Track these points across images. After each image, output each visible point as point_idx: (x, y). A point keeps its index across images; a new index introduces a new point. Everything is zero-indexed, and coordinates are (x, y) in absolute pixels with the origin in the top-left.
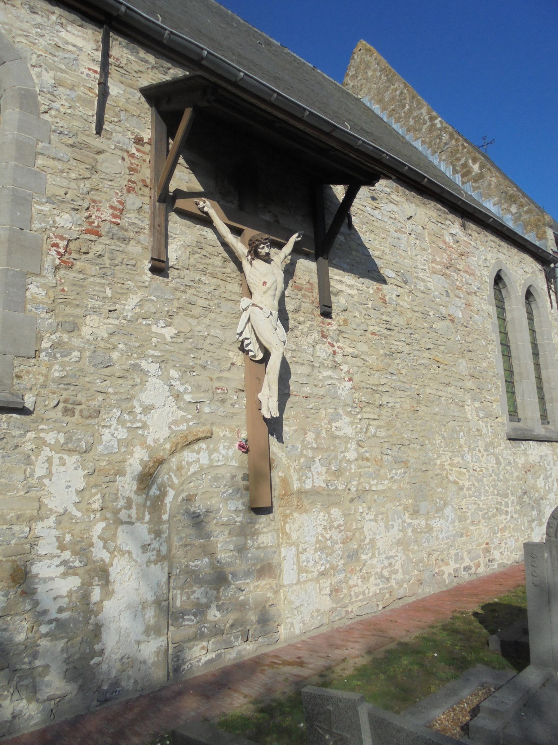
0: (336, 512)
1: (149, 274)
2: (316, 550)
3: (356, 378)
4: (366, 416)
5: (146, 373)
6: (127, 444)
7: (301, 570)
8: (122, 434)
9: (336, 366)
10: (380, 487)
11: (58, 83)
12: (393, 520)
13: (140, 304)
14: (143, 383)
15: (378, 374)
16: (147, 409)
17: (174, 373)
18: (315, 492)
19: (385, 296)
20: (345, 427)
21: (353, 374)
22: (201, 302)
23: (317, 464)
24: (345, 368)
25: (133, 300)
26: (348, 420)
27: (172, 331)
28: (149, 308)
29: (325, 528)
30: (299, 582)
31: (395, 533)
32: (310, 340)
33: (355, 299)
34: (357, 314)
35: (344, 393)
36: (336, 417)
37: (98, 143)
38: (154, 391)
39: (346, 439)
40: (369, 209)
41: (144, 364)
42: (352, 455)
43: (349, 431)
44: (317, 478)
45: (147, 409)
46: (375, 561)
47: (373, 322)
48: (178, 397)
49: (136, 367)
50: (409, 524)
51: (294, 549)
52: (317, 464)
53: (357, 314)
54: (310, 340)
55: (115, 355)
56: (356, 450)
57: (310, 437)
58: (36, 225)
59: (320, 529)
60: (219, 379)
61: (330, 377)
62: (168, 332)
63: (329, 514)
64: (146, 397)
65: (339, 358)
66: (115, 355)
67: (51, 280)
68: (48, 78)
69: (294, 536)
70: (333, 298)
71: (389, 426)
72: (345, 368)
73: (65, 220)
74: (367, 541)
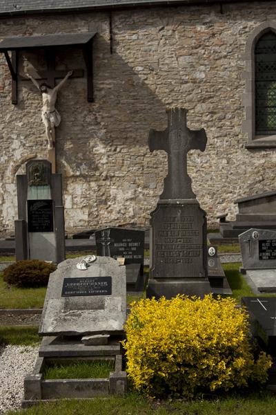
0: (93, 184)
1: (13, 106)
2: (81, 198)
3: (110, 127)
4: (115, 143)
5: (13, 139)
6: (7, 161)
7: (73, 204)
8: (6, 158)
9: (98, 124)
10: (121, 175)
12: (129, 189)
13: (11, 117)
14: (12, 142)
16: (14, 150)
17: (22, 138)
19: (134, 82)
22: (32, 111)
24: (102, 124)
25: (9, 116)
26: (102, 146)
27: (22, 123)
28: (14, 117)
30: (72, 208)
31: (129, 195)
32: (83, 115)
33: (112, 89)
38: (16, 144)
41: (12, 136)
43: (103, 151)
45: (14, 150)
46: (116, 206)
47: (124, 98)
48: (24, 145)
49: (10, 138)
50: (140, 192)
51: (71, 196)
53: (112, 97)
54: (83, 115)
55: (4, 135)
57: (80, 155)
59: (84, 190)
60: (40, 137)
61: (93, 129)
62: (20, 124)
63: (89, 185)
64: (13, 146)
65: (99, 120)
66: (4, 135)
69: (71, 191)
70: (96, 93)
72: (102, 124)
74: (111, 197)
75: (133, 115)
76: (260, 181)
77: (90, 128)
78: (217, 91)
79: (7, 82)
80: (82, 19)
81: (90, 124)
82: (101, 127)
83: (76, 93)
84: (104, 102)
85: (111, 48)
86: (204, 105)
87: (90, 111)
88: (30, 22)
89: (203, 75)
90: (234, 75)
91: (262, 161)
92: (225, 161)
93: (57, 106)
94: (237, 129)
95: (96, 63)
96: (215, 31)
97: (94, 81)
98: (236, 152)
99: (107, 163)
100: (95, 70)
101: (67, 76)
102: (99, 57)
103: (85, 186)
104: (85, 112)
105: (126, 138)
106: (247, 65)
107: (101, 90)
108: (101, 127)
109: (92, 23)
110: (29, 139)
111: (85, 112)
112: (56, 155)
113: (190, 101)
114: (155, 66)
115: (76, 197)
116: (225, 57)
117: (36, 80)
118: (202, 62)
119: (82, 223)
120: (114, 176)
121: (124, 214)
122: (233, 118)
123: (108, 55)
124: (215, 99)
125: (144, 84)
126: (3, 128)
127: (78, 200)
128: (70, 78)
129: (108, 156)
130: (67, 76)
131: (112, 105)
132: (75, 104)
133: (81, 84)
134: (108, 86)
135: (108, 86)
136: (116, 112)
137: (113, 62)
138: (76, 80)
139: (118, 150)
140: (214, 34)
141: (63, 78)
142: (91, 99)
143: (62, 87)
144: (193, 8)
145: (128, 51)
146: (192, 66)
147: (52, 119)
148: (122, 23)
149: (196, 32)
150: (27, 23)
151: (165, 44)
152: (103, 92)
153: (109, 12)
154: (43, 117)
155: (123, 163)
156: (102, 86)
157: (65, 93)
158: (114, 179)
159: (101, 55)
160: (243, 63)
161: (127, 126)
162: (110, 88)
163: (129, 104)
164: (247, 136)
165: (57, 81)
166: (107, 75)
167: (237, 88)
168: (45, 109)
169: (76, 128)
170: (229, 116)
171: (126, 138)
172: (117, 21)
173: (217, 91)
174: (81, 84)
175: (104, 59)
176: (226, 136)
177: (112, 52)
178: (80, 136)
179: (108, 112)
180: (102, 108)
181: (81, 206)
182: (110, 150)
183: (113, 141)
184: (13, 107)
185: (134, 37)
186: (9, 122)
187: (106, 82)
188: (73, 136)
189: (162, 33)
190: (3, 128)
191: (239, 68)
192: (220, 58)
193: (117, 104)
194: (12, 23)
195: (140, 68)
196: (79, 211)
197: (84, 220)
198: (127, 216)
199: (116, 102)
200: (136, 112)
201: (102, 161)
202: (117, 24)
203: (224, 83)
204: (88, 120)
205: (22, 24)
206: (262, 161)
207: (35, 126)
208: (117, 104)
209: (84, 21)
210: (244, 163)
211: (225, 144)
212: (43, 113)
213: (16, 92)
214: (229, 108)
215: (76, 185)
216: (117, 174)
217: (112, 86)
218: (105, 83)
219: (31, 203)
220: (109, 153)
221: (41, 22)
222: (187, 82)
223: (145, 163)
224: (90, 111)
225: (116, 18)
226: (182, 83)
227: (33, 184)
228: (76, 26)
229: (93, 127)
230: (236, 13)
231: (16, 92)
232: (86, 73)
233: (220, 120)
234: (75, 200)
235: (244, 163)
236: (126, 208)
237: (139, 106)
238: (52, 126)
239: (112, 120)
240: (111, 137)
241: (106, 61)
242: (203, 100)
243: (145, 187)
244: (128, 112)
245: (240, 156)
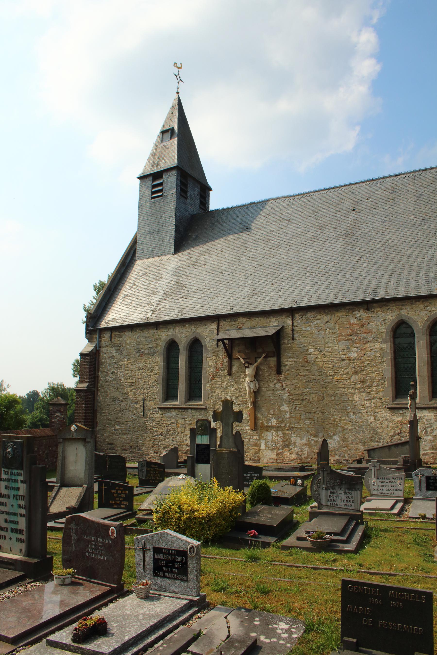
0: (280, 433)
2: (272, 442)
3: (292, 392)
4: (295, 404)
7: (266, 446)
9: (284, 389)
10: (299, 426)
11: (210, 339)
12: (304, 437)
13: (227, 384)
15: (302, 389)
18: (272, 427)
19: (308, 360)
20: (285, 408)
21: (290, 391)
23: (273, 419)
24: (287, 389)
26: (286, 405)
27: (234, 388)
28: (229, 384)
29: (275, 436)
30: (266, 449)
31: (304, 441)
32: (273, 383)
34: (293, 370)
35: (285, 397)
36: (282, 405)
37: (217, 349)
39: (286, 412)
40: (304, 328)
42: (288, 416)
43: (287, 409)
44: (274, 422)
46: (295, 449)
47: (301, 371)
50: (312, 440)
51: (264, 441)
52: (273, 419)
53: (293, 370)
54: (273, 383)
56: (290, 415)
57: (271, 411)
58: (207, 373)
59: (273, 437)
61: (280, 393)
62: (233, 389)
63: (277, 433)
65: (284, 387)
66: (222, 396)
67: (210, 384)
68: (208, 340)
69: (265, 437)
70: (282, 368)
71: (305, 407)
72: (287, 389)
73: (212, 369)
74: (292, 442)
75: (307, 384)
76: (398, 434)
77: (278, 392)
78: (365, 366)
79: (225, 360)
80: (274, 317)
81: (278, 390)
82: (286, 391)
83: (269, 368)
84: (288, 374)
85: (293, 337)
86: (357, 377)
87: (278, 380)
88: (241, 320)
89: (356, 355)
90: (378, 354)
91: (400, 418)
92: (372, 418)
93: (257, 376)
94: (381, 394)
95: (283, 347)
96: (363, 322)
97: (281, 359)
98: (381, 411)
99: (289, 418)
100: (282, 353)
101: (263, 357)
102: (284, 343)
103: (274, 434)
104: (275, 381)
105: (303, 400)
106: (388, 347)
107: (286, 365)
108: (286, 391)
109: (281, 320)
110: (238, 399)
111: (275, 381)
112: (255, 411)
113: (347, 373)
114: (322, 348)
115: (268, 442)
116: (371, 341)
117: (243, 358)
118: (355, 345)
119: (272, 461)
120: (294, 427)
121: (301, 455)
122: (378, 385)
123: (291, 341)
124: (365, 372)
125: (315, 361)
126: (222, 392)
127: (269, 444)
128: (265, 357)
129: (291, 413)
130: (263, 357)
131: (293, 377)
132: (269, 375)
133: (273, 361)
134: (291, 363)
135: (291, 363)
136: (296, 381)
137: (294, 346)
138: (269, 359)
139: (297, 408)
140: (363, 325)
141: (260, 357)
142: (279, 372)
143: (261, 364)
144: (348, 308)
145: (305, 338)
146: (348, 348)
147: (252, 386)
148: (300, 318)
149: (350, 324)
150: (239, 321)
151: (329, 333)
152: (287, 367)
153: (291, 312)
154: (246, 385)
155: (300, 418)
156: (286, 363)
157: (262, 368)
158: (294, 429)
159: (286, 341)
160: (384, 346)
161: (303, 391)
162: (292, 365)
163: (304, 375)
164: (388, 399)
165: (257, 359)
166: (290, 355)
167: (380, 363)
168: (247, 379)
169: (269, 392)
170: (375, 384)
171: (303, 400)
172: (297, 318)
173: (365, 366)
174: (273, 361)
175: (288, 344)
176: (373, 399)
177: (293, 339)
178: (271, 398)
179: (291, 381)
180: (286, 378)
181: (271, 448)
182: (292, 409)
183: (293, 402)
184: (228, 377)
185: (308, 328)
186: (226, 388)
187: (288, 360)
188: (267, 398)
189: (327, 325)
190: (222, 392)
191: (382, 349)
192: (367, 342)
193: (297, 375)
194: (229, 320)
195: (312, 350)
196: (269, 451)
197: (273, 459)
198: (303, 457)
199: (296, 374)
200: (309, 381)
201: (286, 416)
202: (297, 319)
203: (371, 360)
204: (277, 386)
205: (235, 321)
206: (400, 418)
207: (242, 391)
208: (297, 375)
209: (275, 318)
210: (386, 420)
211: (373, 405)
212: (246, 382)
213: (230, 367)
214: (375, 379)
215: (268, 433)
216: (296, 425)
217: (293, 363)
218: (288, 361)
219: (198, 445)
220: (291, 410)
221: (247, 320)
222: (344, 360)
223: (316, 418)
224: (278, 380)
225: (296, 315)
226: (341, 361)
227: (200, 434)
228: (270, 321)
229: (280, 392)
230: (378, 309)
231: (230, 367)
232: (276, 354)
233: (369, 387)
234: (268, 443)
235: (386, 420)
236: (302, 451)
237: (312, 377)
238: (252, 391)
239: (293, 386)
240: (292, 399)
241: (289, 345)
242: (356, 373)
243: (316, 436)
244: (304, 381)
245: (384, 414)
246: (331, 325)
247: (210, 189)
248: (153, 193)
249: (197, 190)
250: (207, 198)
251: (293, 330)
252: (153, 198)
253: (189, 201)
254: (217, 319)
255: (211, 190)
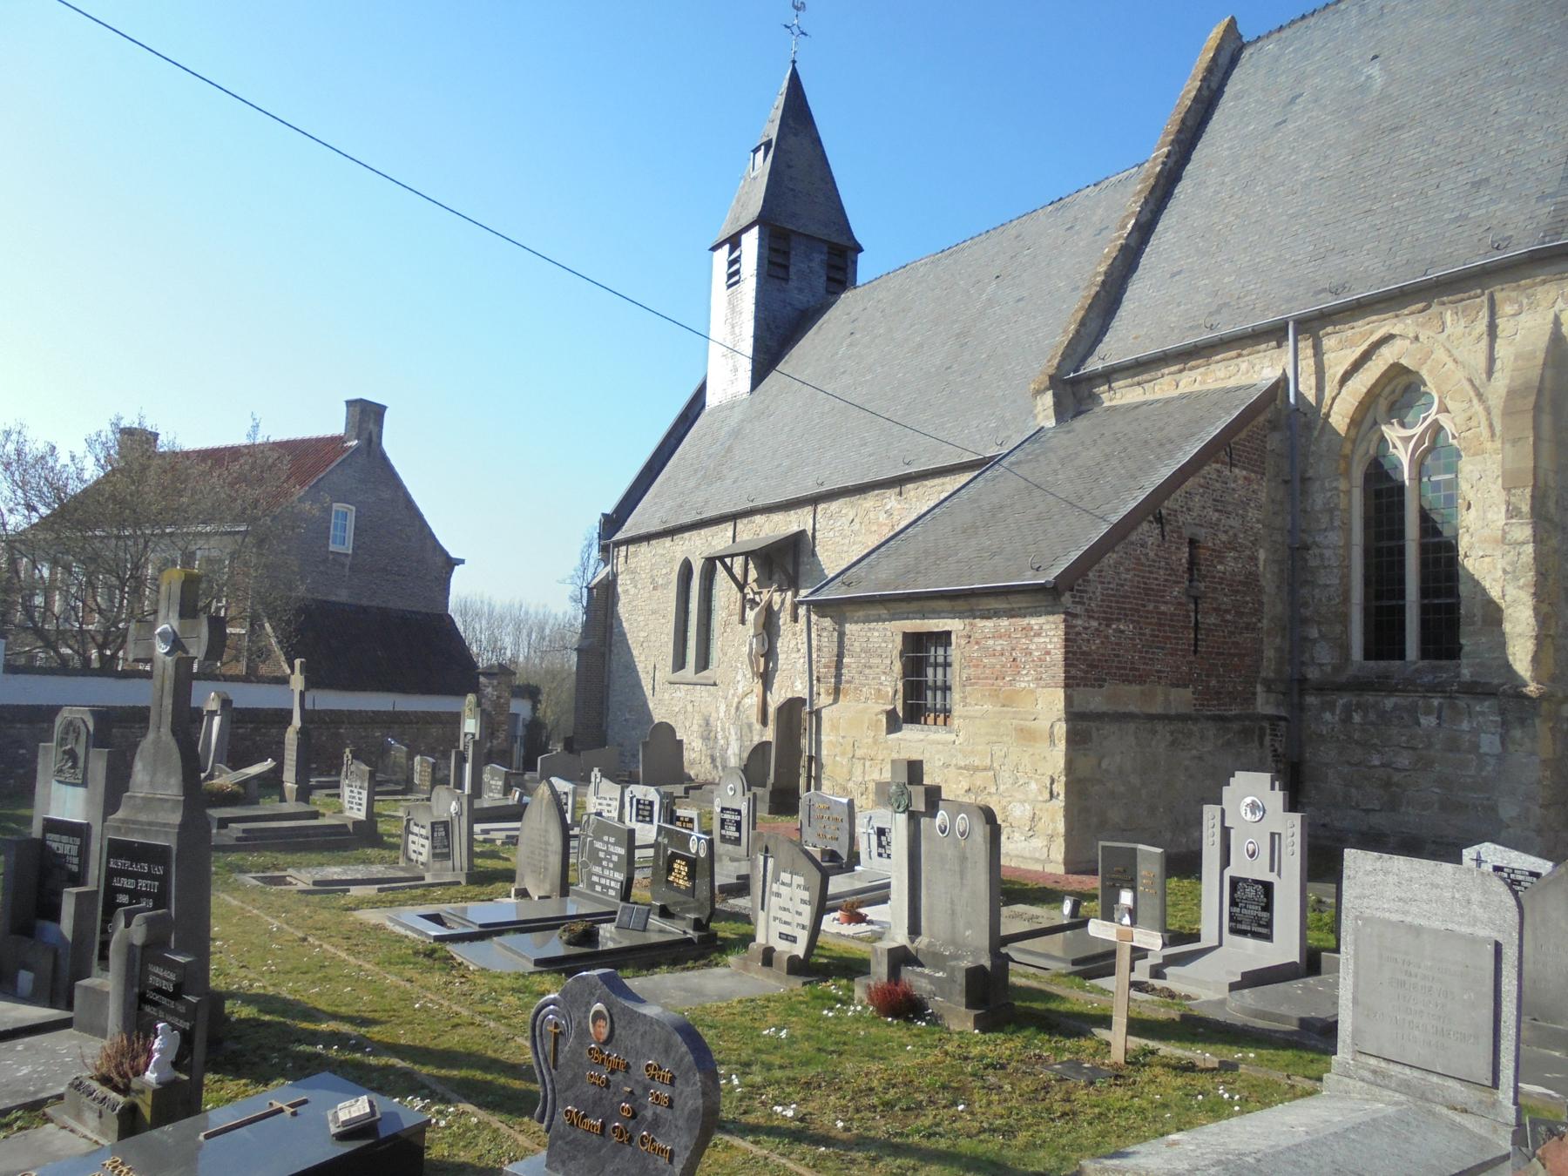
153: (814, 500)
246: (856, 526)
247: (860, 249)
248: (730, 276)
249: (818, 260)
250: (849, 270)
251: (814, 537)
252: (730, 286)
253: (793, 284)
254: (734, 517)
255: (860, 249)
